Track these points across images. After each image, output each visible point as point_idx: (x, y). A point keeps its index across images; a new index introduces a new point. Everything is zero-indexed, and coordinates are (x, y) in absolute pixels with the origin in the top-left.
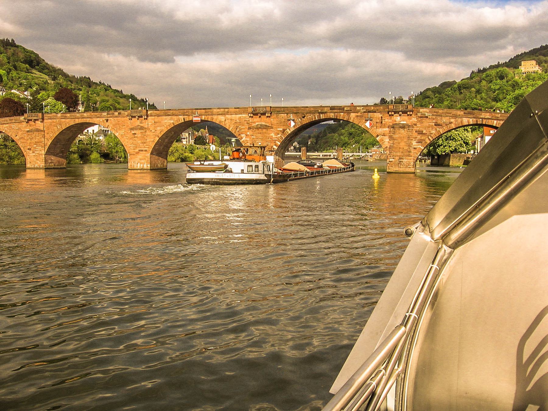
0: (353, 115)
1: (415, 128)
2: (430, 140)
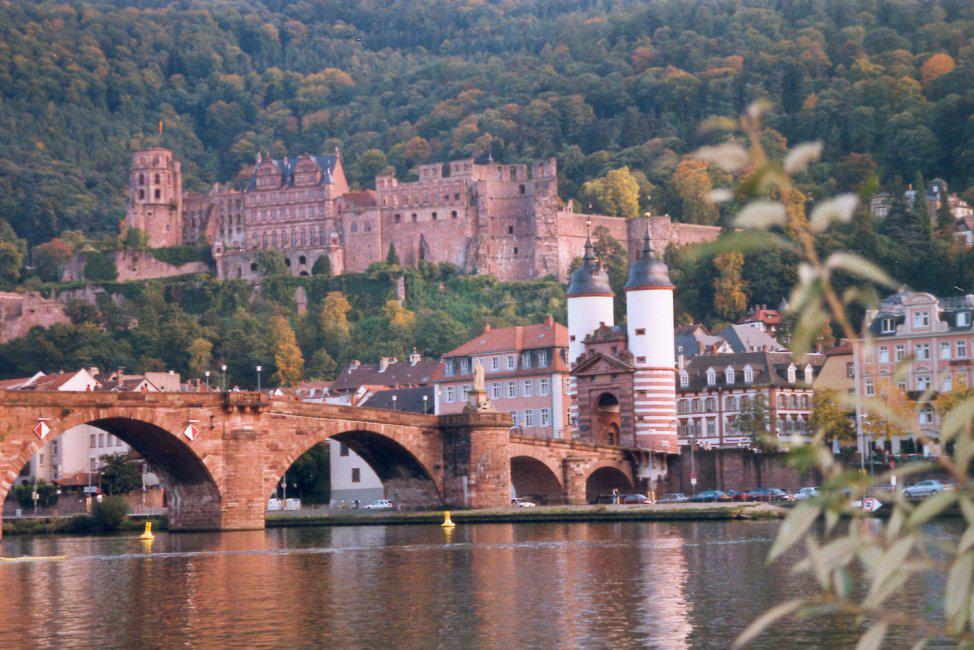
0: (161, 412)
1: (266, 440)
2: (289, 462)
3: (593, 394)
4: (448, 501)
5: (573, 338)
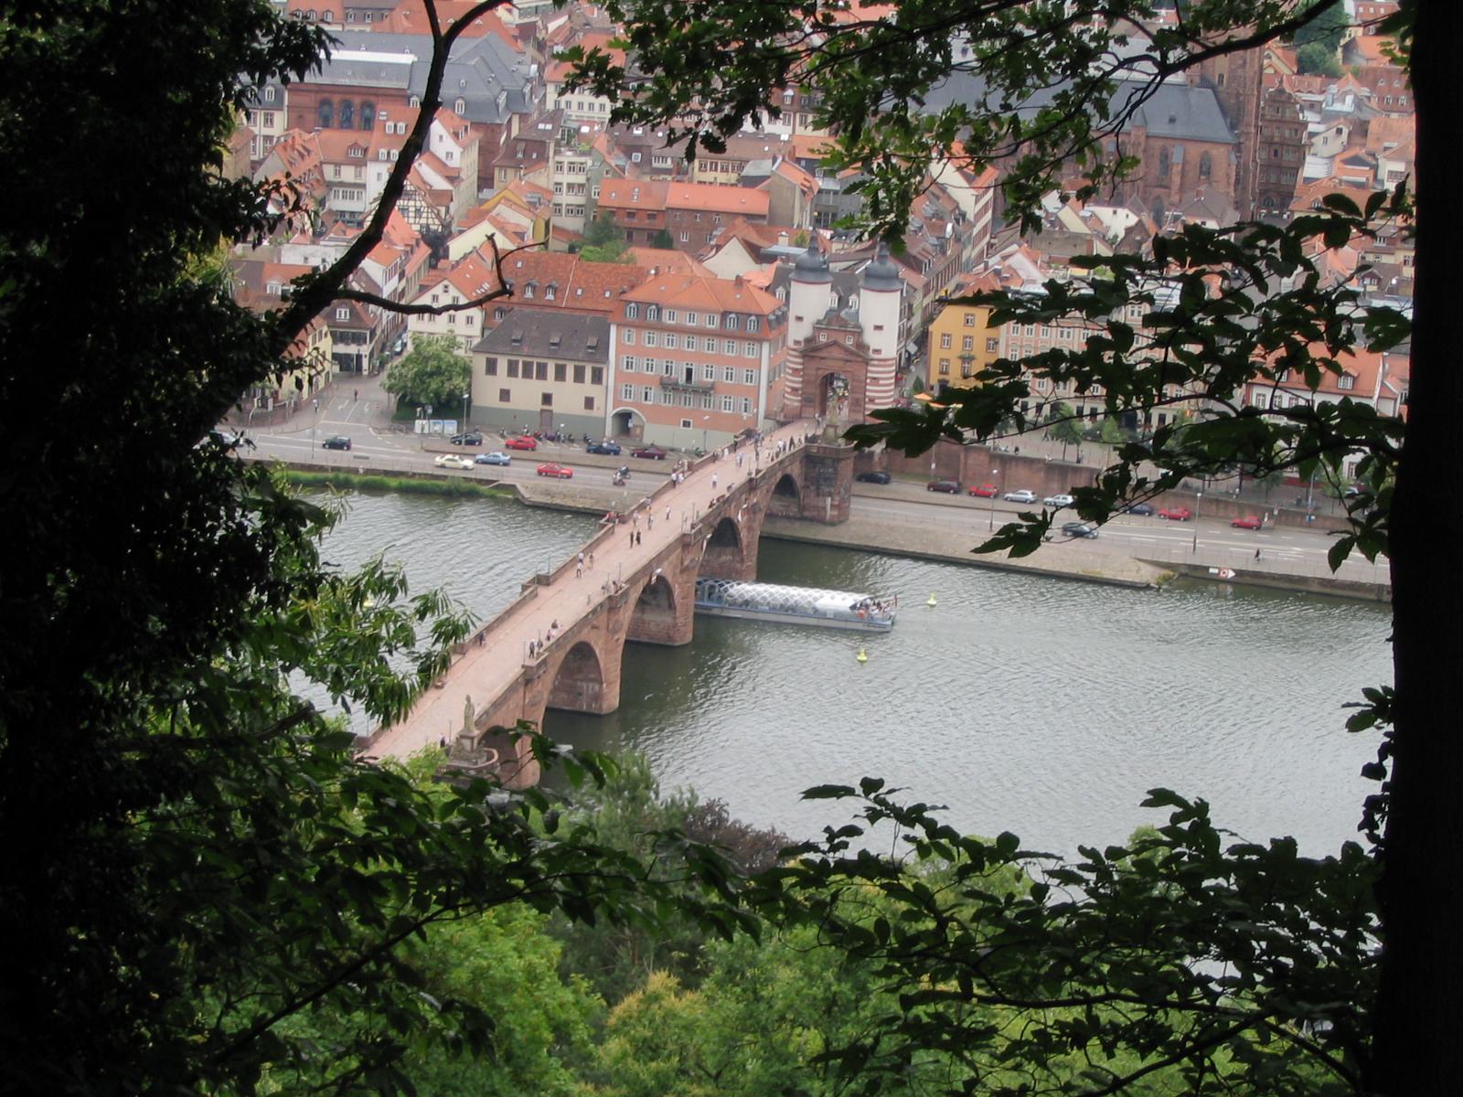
3: (820, 372)
4: (806, 514)
5: (799, 319)
